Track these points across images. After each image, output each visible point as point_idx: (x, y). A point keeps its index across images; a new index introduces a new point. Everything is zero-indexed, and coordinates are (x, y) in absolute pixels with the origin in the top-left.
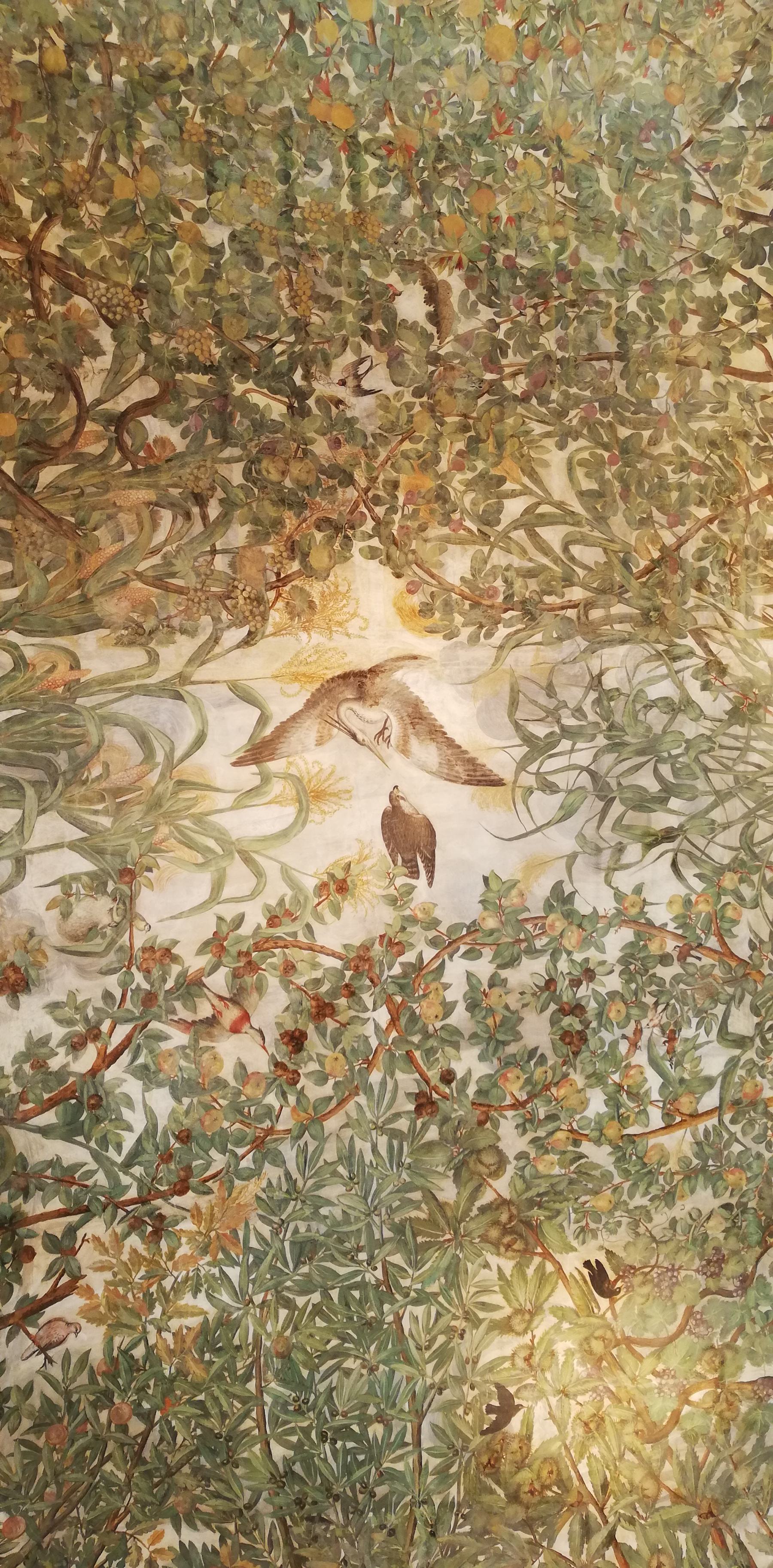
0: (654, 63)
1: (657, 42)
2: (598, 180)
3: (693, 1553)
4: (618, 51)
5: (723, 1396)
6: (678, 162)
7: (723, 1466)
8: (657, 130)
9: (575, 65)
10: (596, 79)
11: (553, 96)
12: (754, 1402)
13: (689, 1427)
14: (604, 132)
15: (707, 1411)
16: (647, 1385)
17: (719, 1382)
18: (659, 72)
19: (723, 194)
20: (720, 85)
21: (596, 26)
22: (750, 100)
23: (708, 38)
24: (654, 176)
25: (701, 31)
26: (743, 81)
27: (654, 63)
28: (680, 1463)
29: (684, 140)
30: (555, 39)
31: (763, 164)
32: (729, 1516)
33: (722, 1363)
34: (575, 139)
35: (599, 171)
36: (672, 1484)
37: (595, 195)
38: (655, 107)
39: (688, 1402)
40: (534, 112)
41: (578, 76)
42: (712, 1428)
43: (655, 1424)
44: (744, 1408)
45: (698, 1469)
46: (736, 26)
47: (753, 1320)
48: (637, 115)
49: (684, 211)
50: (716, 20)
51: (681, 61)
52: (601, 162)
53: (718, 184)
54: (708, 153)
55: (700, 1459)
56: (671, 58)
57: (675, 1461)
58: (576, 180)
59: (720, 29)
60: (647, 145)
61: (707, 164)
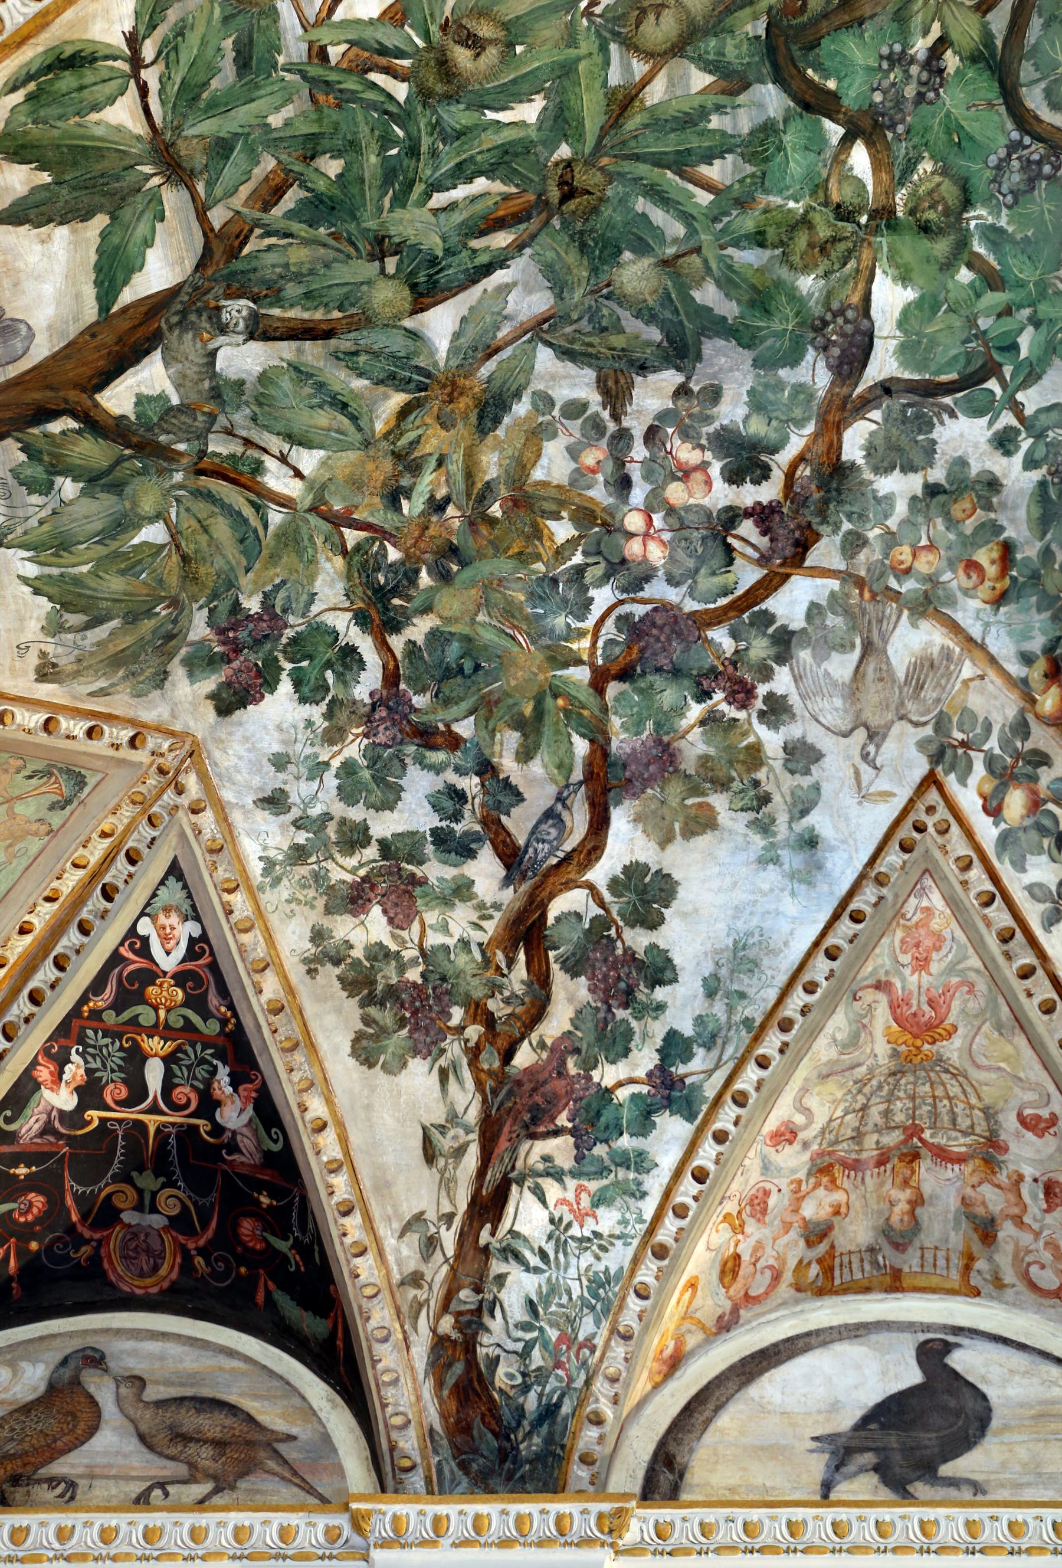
3: (491, 139)
5: (850, 227)
7: (679, 229)
12: (816, 309)
13: (787, 139)
15: (819, 188)
16: (918, 21)
17: (884, 216)
28: (703, 113)
32: (556, 244)
33: (925, 229)
36: (656, 93)
39: (847, 141)
42: (776, 200)
43: (816, 44)
44: (807, 283)
45: (682, 163)
47: (1007, 311)
55: (704, 170)
57: (710, 100)
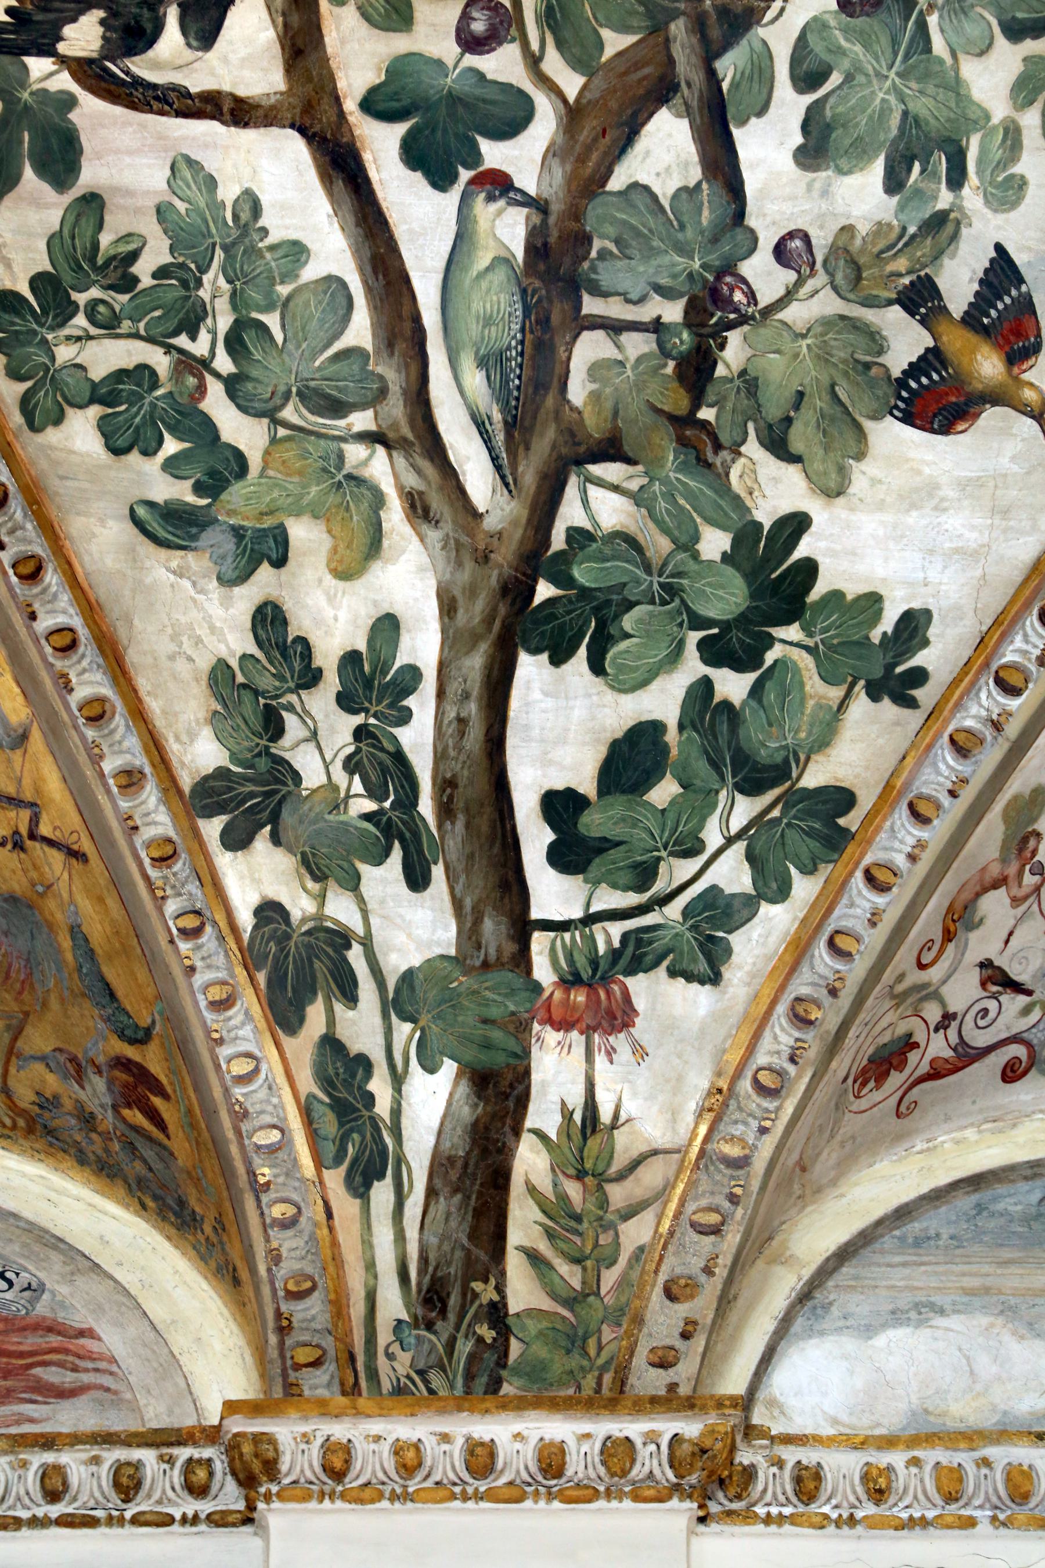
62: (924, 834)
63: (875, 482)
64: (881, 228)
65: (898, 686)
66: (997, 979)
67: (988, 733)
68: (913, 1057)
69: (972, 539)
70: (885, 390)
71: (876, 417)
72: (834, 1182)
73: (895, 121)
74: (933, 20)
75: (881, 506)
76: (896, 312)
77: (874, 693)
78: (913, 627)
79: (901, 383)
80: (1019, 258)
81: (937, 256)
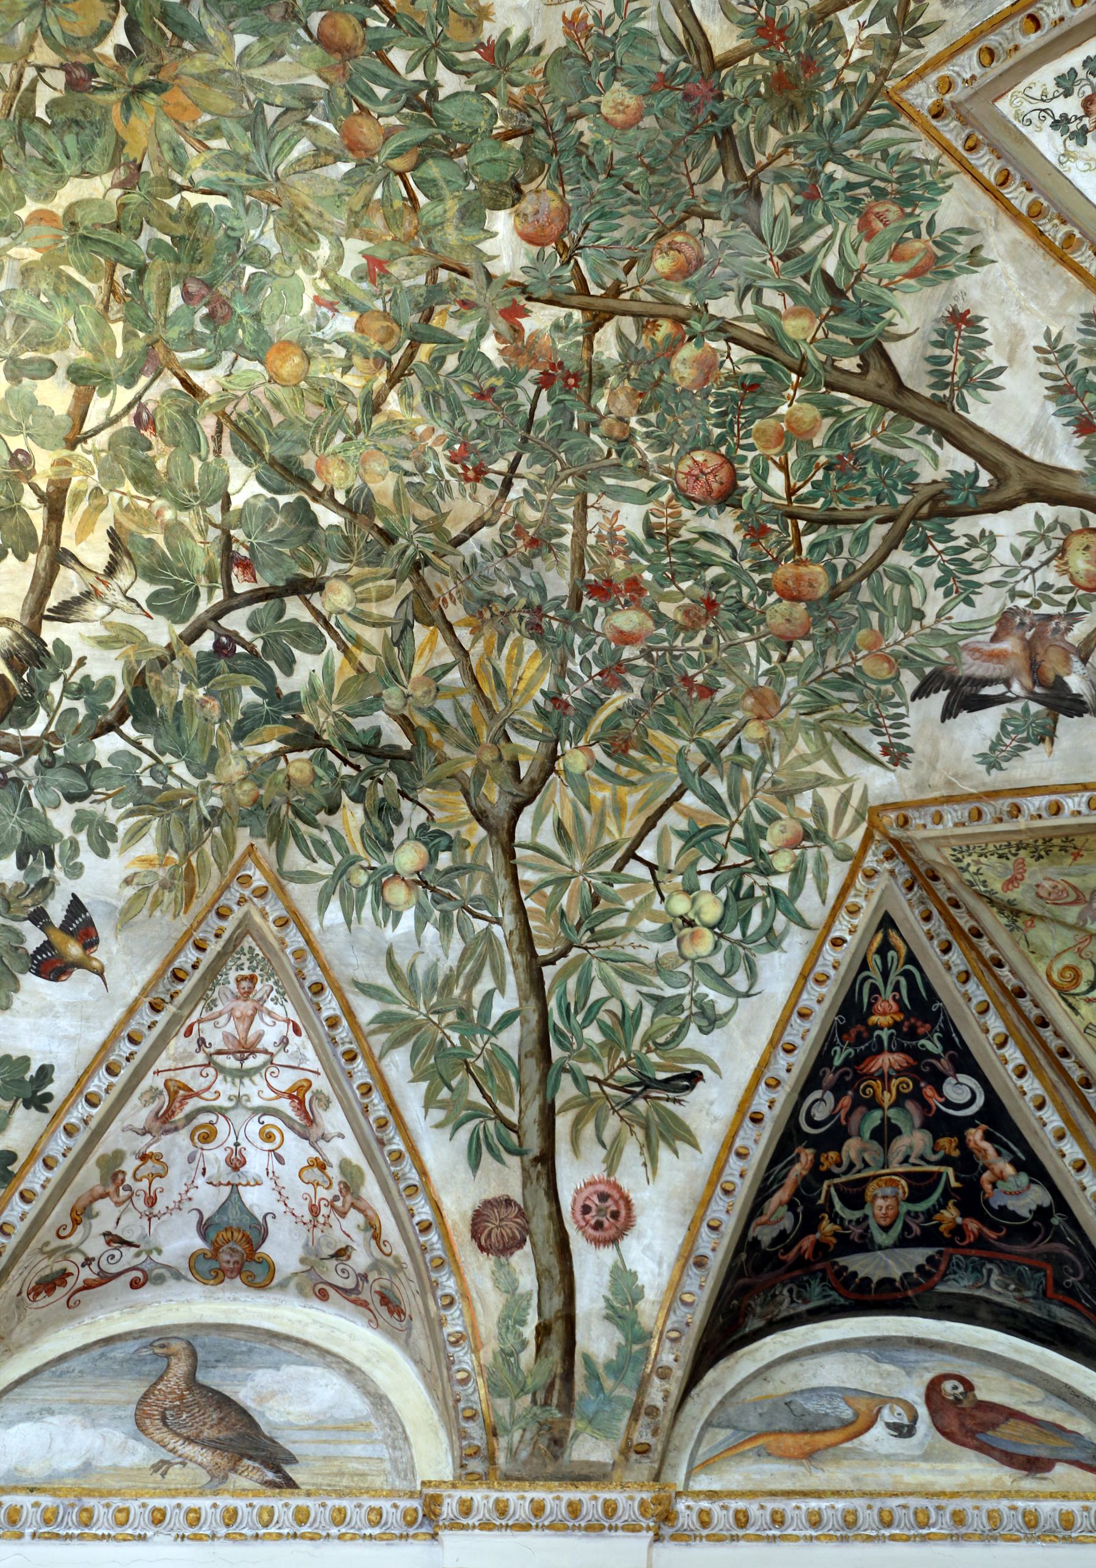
0: (344, 323)
1: (390, 333)
2: (85, 174)
4: (364, 245)
6: (148, 360)
8: (210, 318)
9: (323, 142)
10: (302, 188)
11: (252, 83)
14: (194, 199)
18: (328, 331)
19: (95, 452)
20: (309, 460)
21: (413, 198)
22: (280, 519)
23: (404, 442)
24: (114, 306)
25: (420, 429)
26: (316, 507)
27: (344, 323)
29: (198, 378)
30: (371, 96)
31: (160, 539)
34: (166, 127)
35: (107, 179)
37: (52, 164)
38: (257, 317)
40: (211, 32)
41: (303, 147)
46: (426, 499)
48: (237, 276)
49: (53, 368)
50: (444, 463)
51: (353, 381)
52: (126, 185)
53: (112, 444)
54: (174, 428)
56: (357, 360)
58: (73, 118)
59: (422, 469)
60: (176, 293)
61: (152, 422)
62: (49, 1174)
63: (24, 1003)
64: (17, 885)
65: (38, 1101)
66: (114, 1240)
67: (82, 1126)
68: (70, 1280)
69: (72, 1031)
70: (25, 959)
71: (23, 972)
72: (32, 1342)
73: (19, 836)
74: (32, 792)
75: (27, 1015)
76: (28, 924)
77: (27, 1106)
78: (45, 1073)
79: (34, 957)
80: (84, 901)
81: (45, 898)
